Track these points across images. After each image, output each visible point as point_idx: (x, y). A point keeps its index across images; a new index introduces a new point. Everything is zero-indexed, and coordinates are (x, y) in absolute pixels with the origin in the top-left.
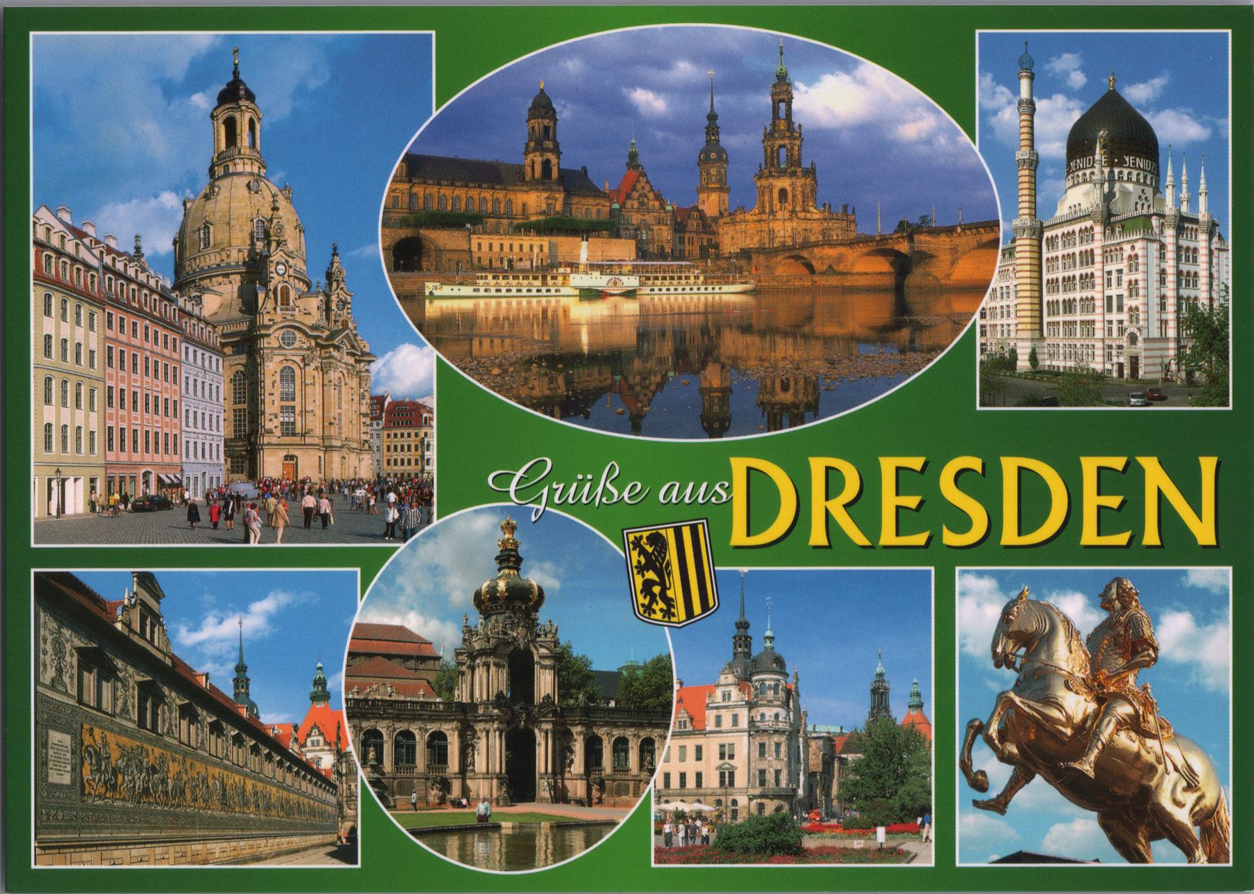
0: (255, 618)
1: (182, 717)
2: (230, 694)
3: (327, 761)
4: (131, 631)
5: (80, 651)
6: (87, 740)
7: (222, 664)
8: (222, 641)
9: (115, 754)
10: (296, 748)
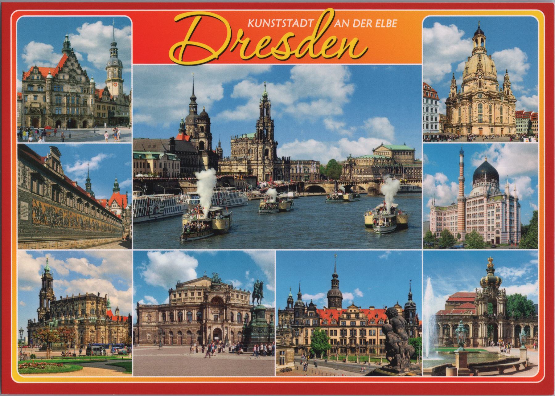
0: (94, 163)
1: (67, 197)
2: (84, 188)
3: (119, 212)
4: (49, 167)
5: (31, 174)
6: (34, 205)
7: (82, 179)
8: (82, 170)
9: (44, 209)
10: (108, 207)
